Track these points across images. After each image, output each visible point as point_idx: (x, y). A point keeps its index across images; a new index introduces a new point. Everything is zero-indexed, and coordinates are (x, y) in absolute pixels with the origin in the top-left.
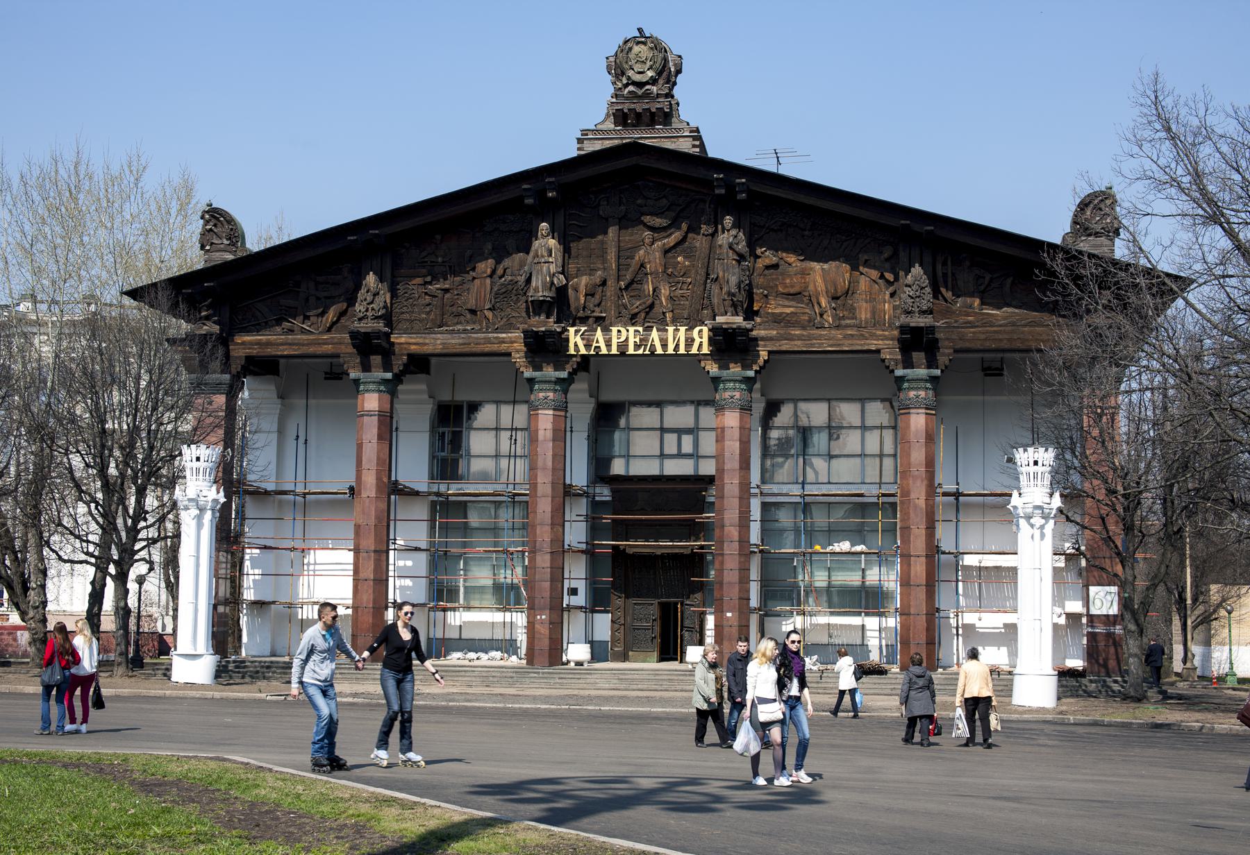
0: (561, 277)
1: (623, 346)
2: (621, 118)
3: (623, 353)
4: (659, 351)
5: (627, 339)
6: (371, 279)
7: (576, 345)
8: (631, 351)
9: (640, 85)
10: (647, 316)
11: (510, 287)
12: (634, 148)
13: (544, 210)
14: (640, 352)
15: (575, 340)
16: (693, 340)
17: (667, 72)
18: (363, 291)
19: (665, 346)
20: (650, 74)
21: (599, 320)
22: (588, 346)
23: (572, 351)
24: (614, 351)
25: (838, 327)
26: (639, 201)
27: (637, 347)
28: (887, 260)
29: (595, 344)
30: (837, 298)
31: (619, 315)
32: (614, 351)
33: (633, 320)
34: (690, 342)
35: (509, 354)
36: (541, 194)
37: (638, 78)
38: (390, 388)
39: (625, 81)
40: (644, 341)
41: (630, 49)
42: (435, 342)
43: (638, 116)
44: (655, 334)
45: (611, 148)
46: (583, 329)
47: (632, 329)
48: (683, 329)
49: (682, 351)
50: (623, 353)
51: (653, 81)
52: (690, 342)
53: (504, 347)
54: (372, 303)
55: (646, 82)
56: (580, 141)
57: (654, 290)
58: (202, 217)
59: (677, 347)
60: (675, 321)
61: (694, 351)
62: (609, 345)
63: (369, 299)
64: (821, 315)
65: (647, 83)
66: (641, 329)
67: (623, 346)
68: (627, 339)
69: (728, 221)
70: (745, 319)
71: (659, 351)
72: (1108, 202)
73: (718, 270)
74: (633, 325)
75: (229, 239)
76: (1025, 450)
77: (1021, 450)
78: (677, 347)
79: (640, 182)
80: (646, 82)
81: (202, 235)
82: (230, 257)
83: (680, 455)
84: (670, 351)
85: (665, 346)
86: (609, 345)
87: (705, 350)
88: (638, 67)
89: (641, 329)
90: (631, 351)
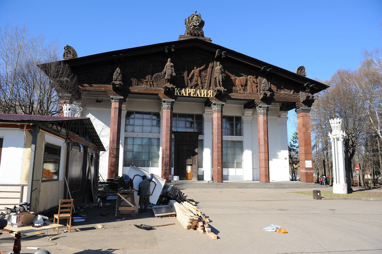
0: (174, 73)
1: (190, 94)
3: (189, 96)
4: (199, 96)
5: (191, 92)
6: (118, 70)
7: (177, 94)
8: (192, 95)
9: (195, 26)
11: (158, 76)
13: (170, 55)
14: (194, 96)
15: (177, 91)
16: (208, 94)
18: (116, 72)
19: (201, 94)
20: (198, 24)
23: (176, 94)
24: (187, 95)
25: (244, 93)
26: (193, 57)
27: (193, 95)
28: (255, 78)
29: (182, 93)
30: (243, 86)
32: (187, 95)
33: (191, 88)
34: (207, 95)
35: (157, 95)
36: (170, 50)
37: (195, 24)
39: (191, 25)
40: (195, 93)
41: (194, 16)
44: (198, 92)
45: (192, 39)
46: (179, 89)
47: (192, 90)
48: (206, 91)
49: (205, 96)
50: (189, 96)
51: (198, 26)
52: (207, 95)
54: (119, 76)
56: (180, 38)
57: (197, 80)
58: (65, 48)
59: (204, 95)
61: (209, 96)
62: (186, 94)
63: (118, 75)
64: (240, 90)
65: (197, 26)
66: (195, 90)
67: (190, 94)
68: (191, 92)
69: (218, 63)
70: (224, 88)
71: (199, 96)
72: (304, 69)
74: (192, 89)
75: (73, 55)
76: (333, 119)
77: (332, 119)
78: (204, 95)
79: (193, 52)
81: (64, 54)
84: (202, 96)
85: (201, 94)
86: (186, 94)
87: (212, 96)
88: (195, 22)
89: (195, 90)
90: (192, 95)
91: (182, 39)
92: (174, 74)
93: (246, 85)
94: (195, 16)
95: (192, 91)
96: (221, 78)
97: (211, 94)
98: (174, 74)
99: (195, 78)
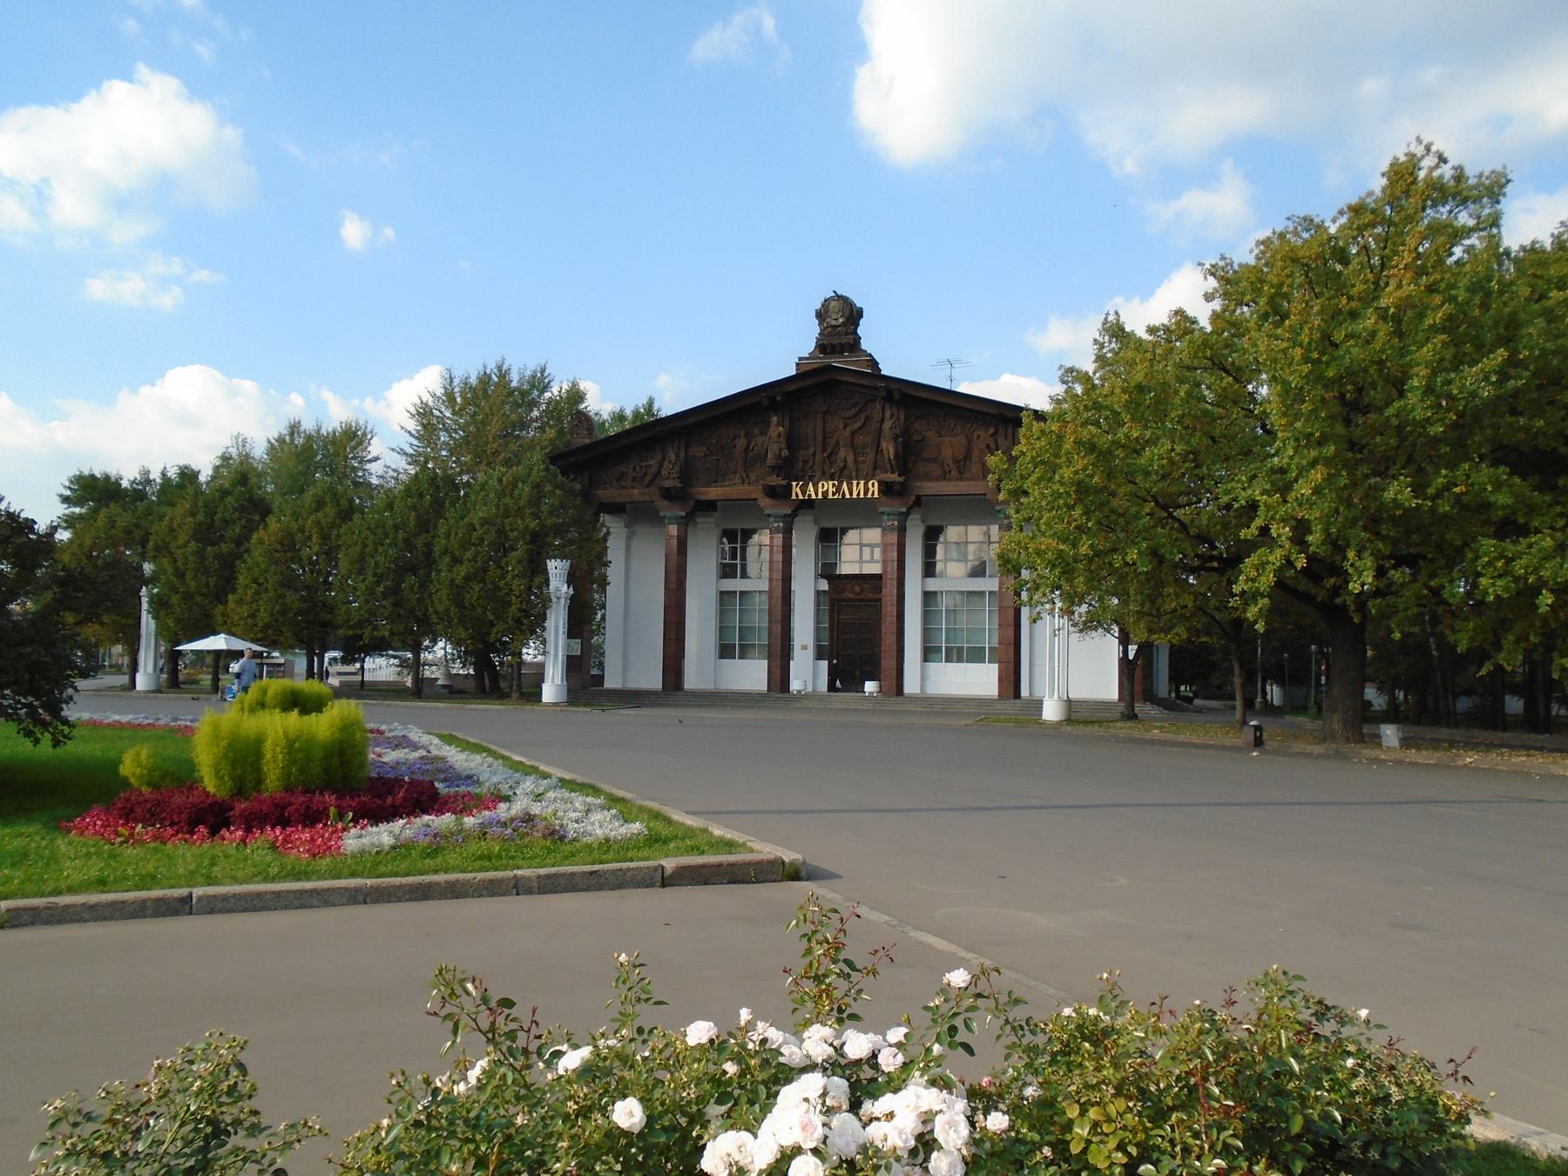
1: (825, 493)
2: (823, 347)
9: (835, 327)
10: (841, 475)
12: (829, 368)
13: (774, 407)
15: (796, 490)
17: (854, 315)
21: (811, 478)
22: (804, 493)
31: (824, 474)
34: (866, 490)
38: (686, 522)
40: (838, 490)
42: (712, 493)
43: (833, 346)
52: (866, 490)
53: (753, 496)
55: (839, 324)
60: (857, 478)
67: (825, 493)
73: (884, 445)
80: (839, 324)
82: (588, 441)
83: (872, 561)
91: (804, 369)
92: (785, 453)
93: (968, 456)
94: (833, 304)
95: (828, 486)
96: (892, 452)
97: (874, 488)
98: (785, 453)
99: (842, 453)
